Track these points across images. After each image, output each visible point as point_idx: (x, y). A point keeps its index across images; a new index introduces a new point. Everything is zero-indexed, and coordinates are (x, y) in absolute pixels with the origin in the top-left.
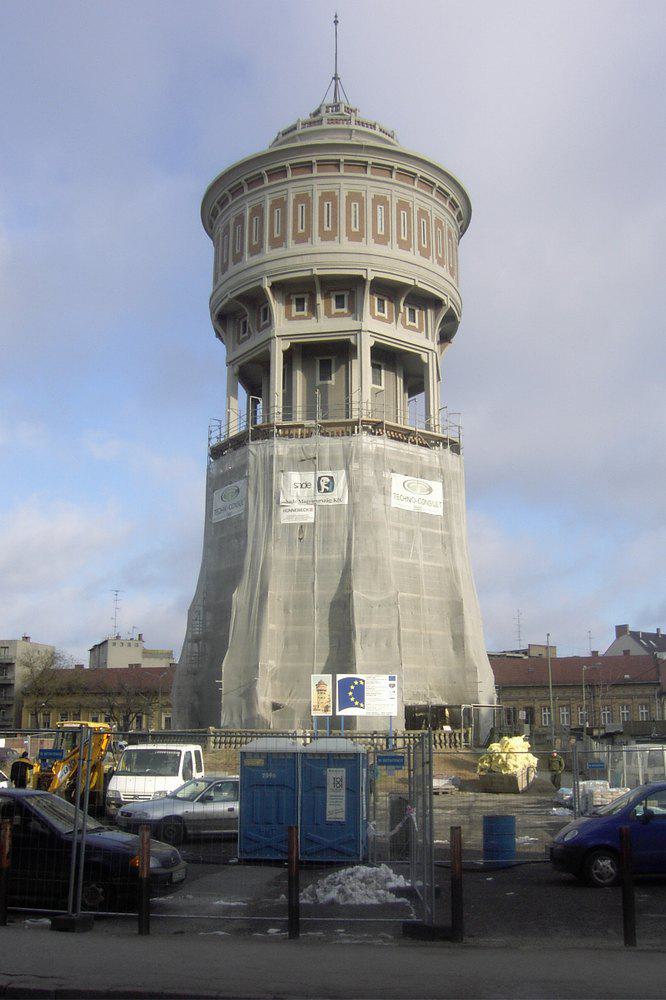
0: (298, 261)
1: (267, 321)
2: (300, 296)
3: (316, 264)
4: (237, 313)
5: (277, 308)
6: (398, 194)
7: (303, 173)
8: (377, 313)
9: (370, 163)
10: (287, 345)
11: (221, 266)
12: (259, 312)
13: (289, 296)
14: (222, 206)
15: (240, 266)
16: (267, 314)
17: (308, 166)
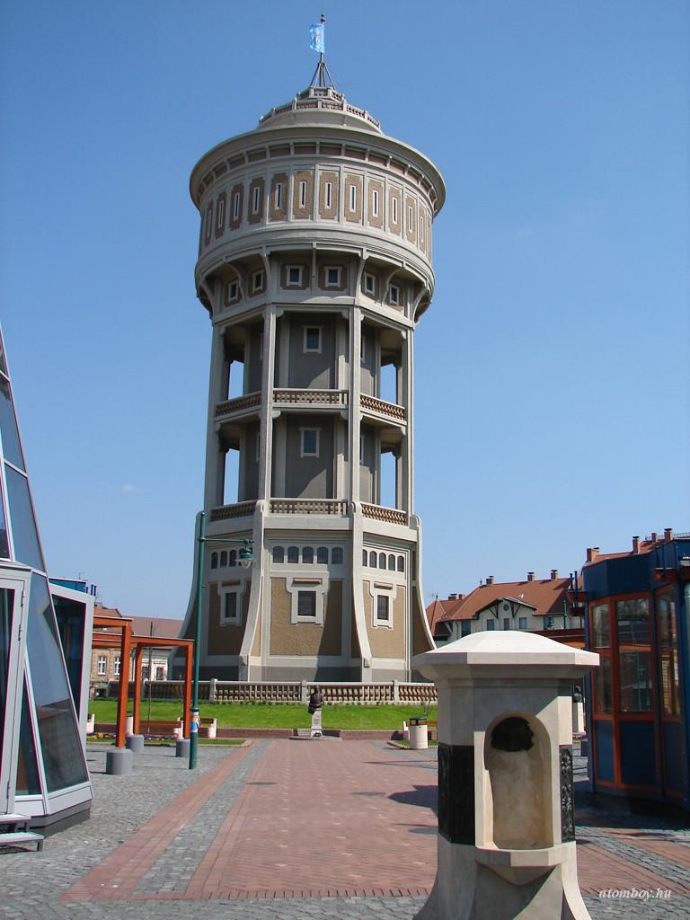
0: (302, 235)
1: (261, 288)
2: (296, 267)
3: (316, 239)
4: (217, 283)
5: (273, 277)
6: (391, 182)
7: (258, 159)
8: (366, 290)
9: (344, 145)
10: (281, 313)
11: (205, 241)
12: (251, 279)
13: (285, 264)
14: (208, 183)
15: (222, 240)
16: (260, 280)
17: (286, 149)
